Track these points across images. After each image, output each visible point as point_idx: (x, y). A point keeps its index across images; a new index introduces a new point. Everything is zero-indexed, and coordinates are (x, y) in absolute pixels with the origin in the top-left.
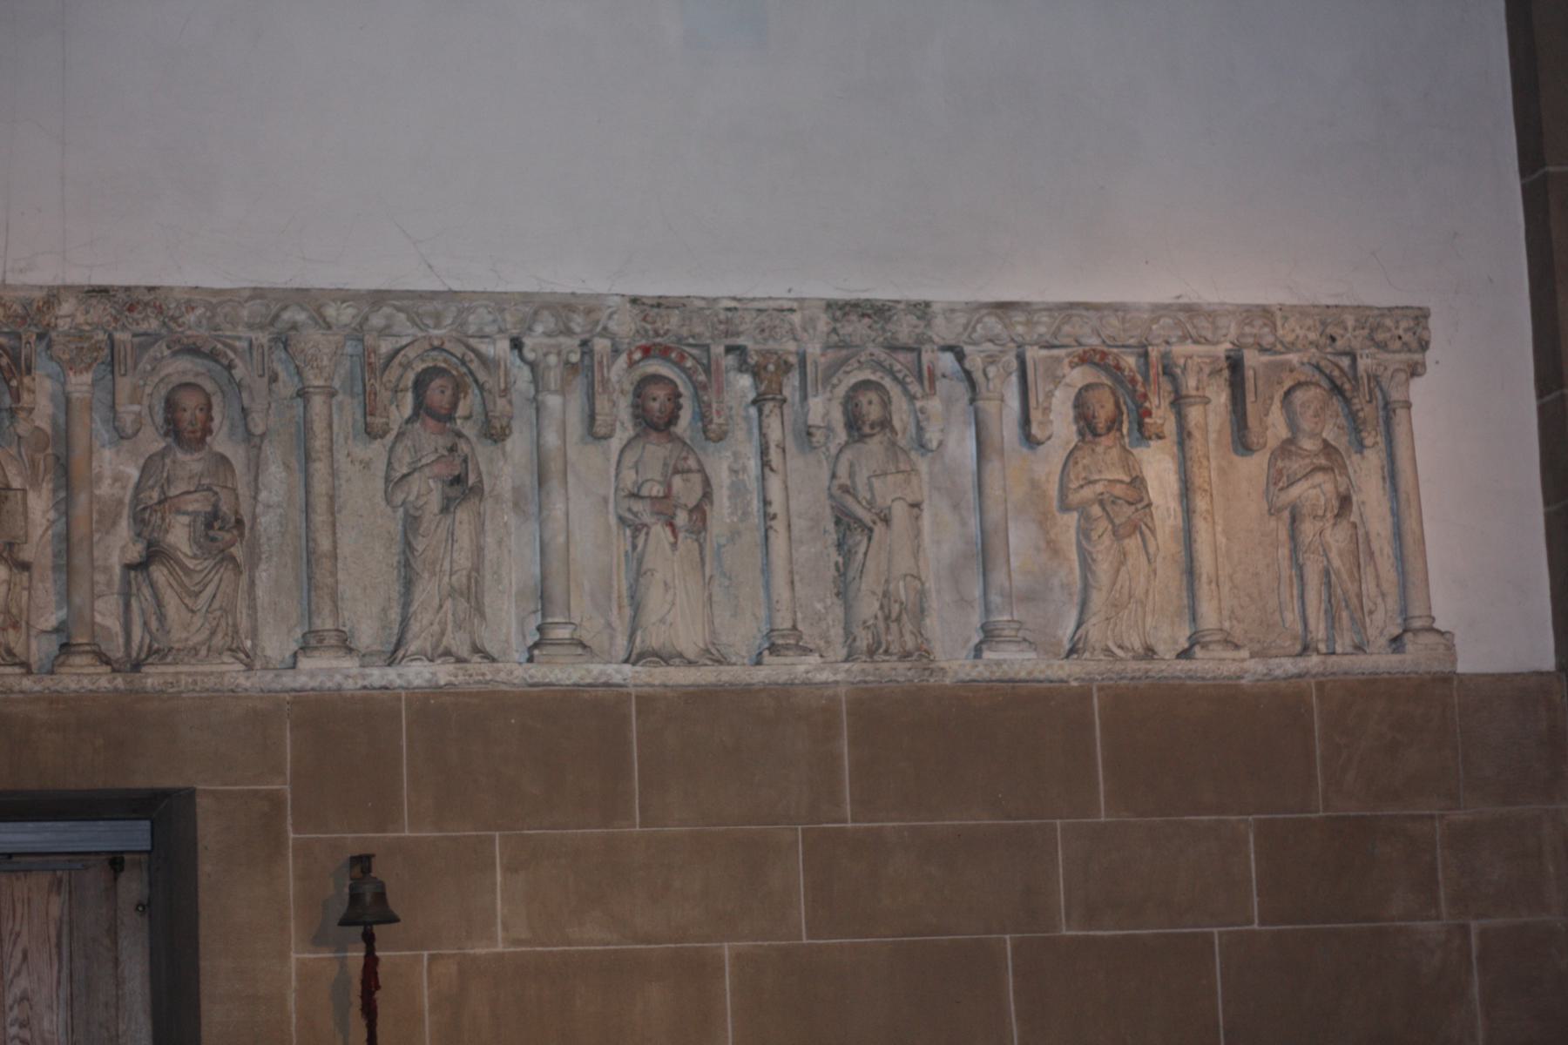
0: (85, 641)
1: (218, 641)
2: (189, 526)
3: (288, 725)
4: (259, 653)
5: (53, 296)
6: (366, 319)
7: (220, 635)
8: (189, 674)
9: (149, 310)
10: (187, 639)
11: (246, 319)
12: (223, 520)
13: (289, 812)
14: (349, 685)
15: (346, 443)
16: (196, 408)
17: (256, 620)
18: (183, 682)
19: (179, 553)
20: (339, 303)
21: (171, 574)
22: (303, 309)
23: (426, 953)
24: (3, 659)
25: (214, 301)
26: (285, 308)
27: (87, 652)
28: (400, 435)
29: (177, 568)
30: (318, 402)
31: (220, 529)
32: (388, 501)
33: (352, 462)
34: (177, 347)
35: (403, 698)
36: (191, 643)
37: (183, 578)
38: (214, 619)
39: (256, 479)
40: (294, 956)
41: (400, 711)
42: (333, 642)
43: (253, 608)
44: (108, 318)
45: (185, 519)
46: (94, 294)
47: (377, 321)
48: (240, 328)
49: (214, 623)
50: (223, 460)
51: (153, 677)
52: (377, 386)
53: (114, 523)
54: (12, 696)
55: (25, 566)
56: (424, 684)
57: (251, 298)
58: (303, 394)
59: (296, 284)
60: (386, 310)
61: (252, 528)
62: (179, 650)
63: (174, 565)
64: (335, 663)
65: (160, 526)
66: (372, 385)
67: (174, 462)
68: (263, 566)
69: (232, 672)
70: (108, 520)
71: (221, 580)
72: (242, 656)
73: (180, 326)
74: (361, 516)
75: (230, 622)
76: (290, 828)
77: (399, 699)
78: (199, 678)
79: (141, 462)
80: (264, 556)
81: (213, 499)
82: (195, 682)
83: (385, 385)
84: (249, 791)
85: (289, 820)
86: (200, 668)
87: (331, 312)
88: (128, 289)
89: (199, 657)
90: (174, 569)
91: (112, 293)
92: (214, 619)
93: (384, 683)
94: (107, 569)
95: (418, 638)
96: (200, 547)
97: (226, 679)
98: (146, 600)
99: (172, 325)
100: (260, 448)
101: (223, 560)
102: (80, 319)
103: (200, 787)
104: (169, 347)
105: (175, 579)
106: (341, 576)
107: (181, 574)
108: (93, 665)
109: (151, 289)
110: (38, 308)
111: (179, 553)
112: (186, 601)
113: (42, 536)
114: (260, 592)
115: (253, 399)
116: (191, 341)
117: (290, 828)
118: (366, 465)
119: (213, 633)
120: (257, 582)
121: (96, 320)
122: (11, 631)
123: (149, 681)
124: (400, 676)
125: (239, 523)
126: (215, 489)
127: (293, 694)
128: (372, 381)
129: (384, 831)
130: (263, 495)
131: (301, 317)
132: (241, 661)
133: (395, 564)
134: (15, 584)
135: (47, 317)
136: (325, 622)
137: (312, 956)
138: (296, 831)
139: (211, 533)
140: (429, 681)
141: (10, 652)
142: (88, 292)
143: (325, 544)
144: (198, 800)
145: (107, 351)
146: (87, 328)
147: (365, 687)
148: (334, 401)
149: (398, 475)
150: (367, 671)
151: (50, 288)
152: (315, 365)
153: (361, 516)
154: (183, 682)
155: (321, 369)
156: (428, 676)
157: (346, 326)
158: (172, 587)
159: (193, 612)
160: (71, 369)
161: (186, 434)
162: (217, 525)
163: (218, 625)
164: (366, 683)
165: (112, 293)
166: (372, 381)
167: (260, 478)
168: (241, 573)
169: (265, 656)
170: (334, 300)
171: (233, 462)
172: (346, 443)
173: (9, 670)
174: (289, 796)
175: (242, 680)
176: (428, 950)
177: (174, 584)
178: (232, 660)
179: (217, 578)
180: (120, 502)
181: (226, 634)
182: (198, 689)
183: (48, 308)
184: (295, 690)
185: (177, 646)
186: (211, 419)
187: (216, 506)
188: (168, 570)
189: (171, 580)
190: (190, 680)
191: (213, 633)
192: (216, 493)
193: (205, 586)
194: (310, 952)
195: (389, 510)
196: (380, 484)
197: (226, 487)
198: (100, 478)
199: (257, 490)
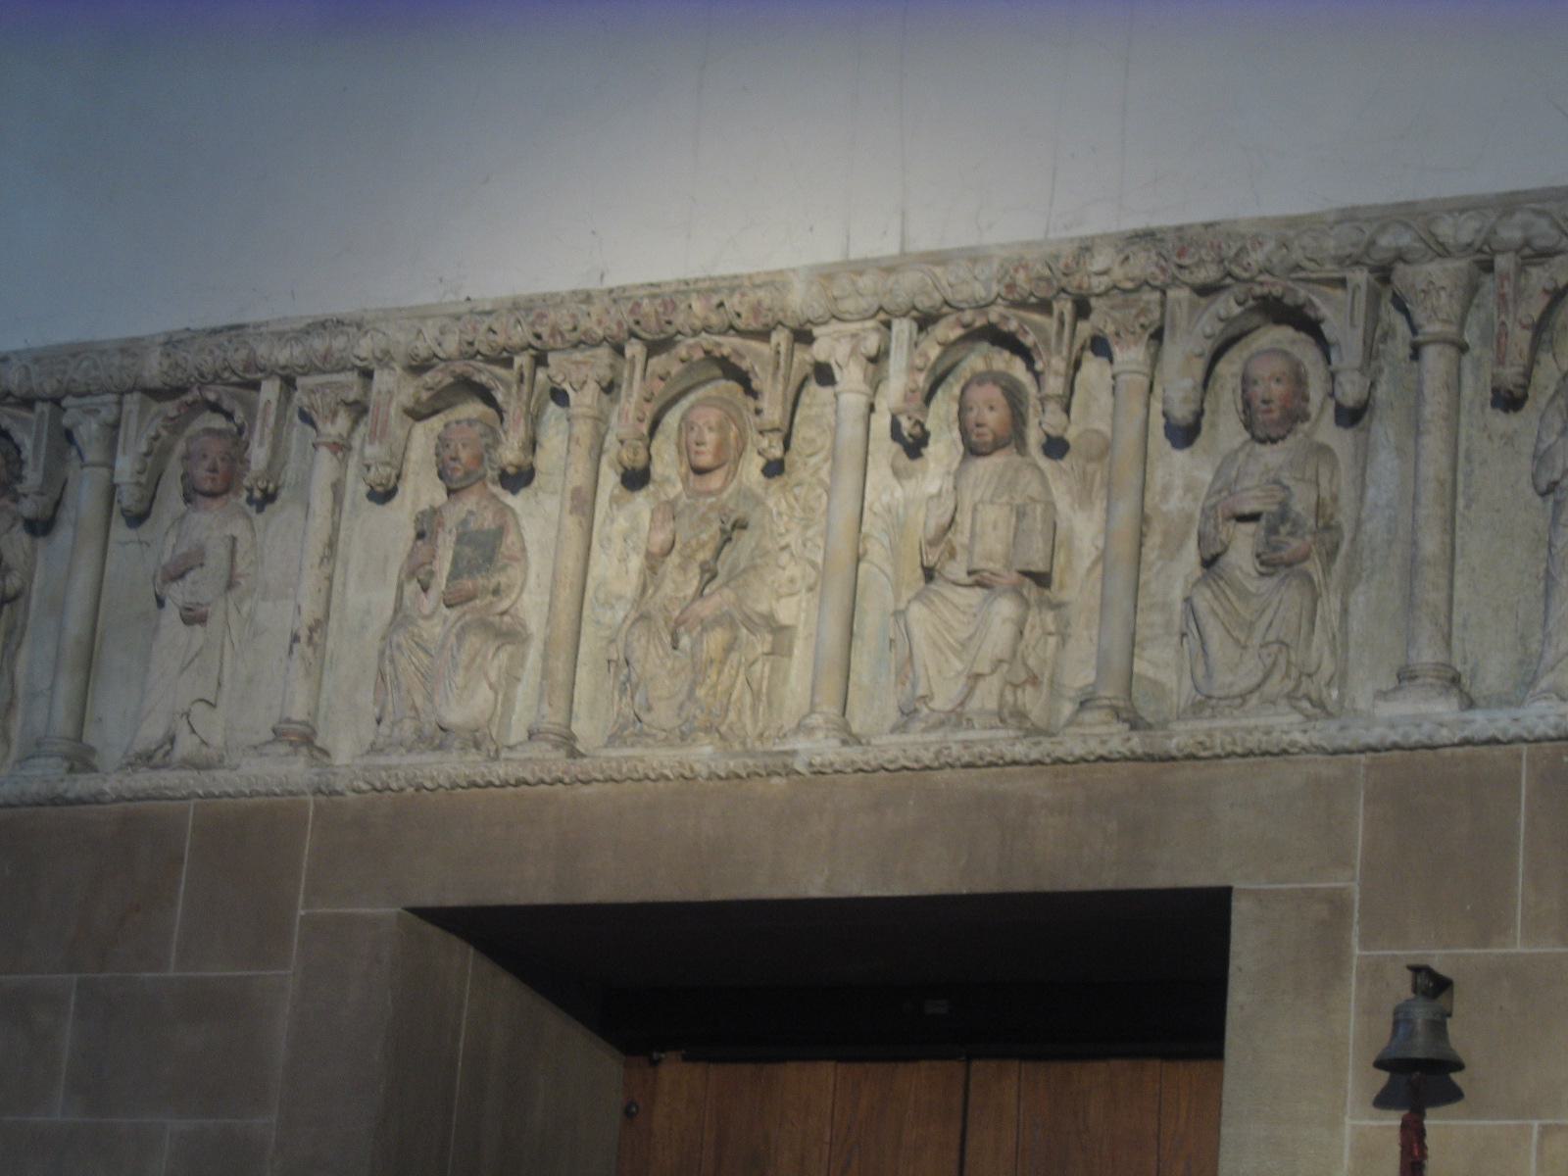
0: (1109, 693)
1: (1274, 685)
2: (1254, 535)
3: (1362, 801)
4: (1346, 704)
5: (1086, 248)
6: (1493, 231)
7: (1276, 677)
8: (1226, 731)
9: (1203, 252)
10: (1231, 685)
11: (1333, 252)
12: (1295, 524)
13: (1356, 915)
14: (1444, 735)
15: (1483, 412)
16: (1270, 378)
17: (1347, 660)
18: (1218, 741)
19: (1238, 573)
20: (1457, 214)
21: (1216, 597)
22: (1407, 226)
23: (1536, 1123)
24: (1002, 721)
25: (1291, 233)
26: (1383, 228)
27: (1100, 707)
28: (1557, 392)
29: (1228, 592)
30: (1430, 353)
31: (1291, 534)
32: (1535, 486)
33: (1490, 437)
34: (1251, 303)
35: (1524, 757)
36: (1236, 690)
37: (1237, 604)
38: (1269, 655)
39: (1363, 475)
40: (1348, 1121)
41: (1518, 773)
42: (1430, 680)
43: (1340, 642)
44: (1153, 269)
45: (1249, 528)
46: (1138, 240)
47: (1511, 233)
48: (1328, 267)
49: (1269, 661)
50: (1324, 450)
51: (1180, 737)
52: (1509, 326)
53: (1181, 545)
54: (1008, 769)
55: (1057, 606)
56: (1552, 733)
57: (1339, 222)
58: (1416, 352)
59: (1402, 199)
60: (1519, 218)
61: (1354, 540)
62: (1220, 699)
63: (1228, 592)
64: (1423, 708)
65: (1215, 539)
66: (1503, 324)
67: (1249, 455)
68: (1361, 588)
69: (1286, 725)
70: (1172, 548)
71: (1280, 602)
72: (1305, 704)
73: (1246, 270)
74: (1498, 511)
75: (1293, 658)
76: (1355, 941)
77: (1519, 757)
78: (1238, 735)
79: (1218, 463)
80: (1364, 575)
81: (1280, 495)
82: (1234, 743)
83: (1520, 322)
84: (1304, 890)
85: (1356, 929)
86: (1244, 722)
87: (1445, 230)
88: (1180, 229)
89: (1246, 708)
90: (1224, 592)
91: (1159, 236)
92: (1269, 655)
93: (1492, 731)
94: (1165, 606)
95: (1553, 669)
96: (1262, 563)
97: (1275, 735)
98: (1194, 637)
99: (1237, 270)
100: (1369, 431)
101: (1287, 576)
102: (1118, 273)
103: (1237, 885)
104: (1240, 304)
105: (1221, 604)
106: (1461, 593)
107: (1233, 598)
108: (1106, 723)
109: (1208, 226)
110: (1067, 266)
111: (1238, 573)
112: (1236, 634)
113: (1090, 570)
114: (1355, 625)
115: (1341, 359)
116: (1266, 290)
117: (1355, 941)
118: (1509, 439)
119: (1266, 677)
120: (1352, 609)
121: (1137, 272)
122: (1029, 689)
123: (1175, 741)
124: (1516, 720)
125: (1326, 524)
126: (1286, 482)
127: (1370, 754)
128: (1503, 317)
129: (1485, 946)
130: (1371, 493)
131: (1406, 240)
132: (1301, 711)
133: (1542, 574)
134: (1033, 627)
135: (1078, 277)
136: (1427, 654)
137: (1374, 1123)
138: (1365, 943)
139: (1273, 538)
140: (1556, 727)
141: (1020, 715)
142: (1131, 237)
143: (1431, 544)
144: (1234, 904)
145: (1157, 314)
146: (1129, 285)
147: (1466, 742)
148: (1466, 360)
149: (1543, 446)
150: (1468, 715)
151: (1081, 239)
152: (1429, 306)
153: (1498, 511)
154: (1218, 741)
155: (1434, 311)
156: (1552, 720)
157: (1469, 245)
158: (1216, 615)
159: (1245, 647)
160: (1117, 343)
161: (1260, 416)
162: (1283, 530)
163: (1274, 664)
164: (1467, 733)
165: (1159, 236)
166: (1503, 317)
167: (1368, 471)
168: (1315, 598)
169: (1355, 710)
170: (1450, 212)
171: (1336, 450)
172: (1483, 412)
173: (1001, 733)
174: (1357, 897)
175: (1298, 737)
176: (1538, 1117)
177: (1220, 612)
178: (1288, 709)
179: (1277, 600)
180: (1189, 518)
181: (1287, 675)
182: (1239, 750)
183: (1078, 263)
184: (1375, 750)
185: (1216, 693)
186: (1306, 399)
187: (1284, 505)
188: (1213, 592)
189: (1216, 606)
190: (1228, 739)
191: (1266, 677)
192: (1286, 488)
193: (1264, 611)
194: (1372, 1118)
195: (1538, 500)
196: (1526, 464)
197: (1302, 480)
198: (1166, 490)
199: (1363, 487)
